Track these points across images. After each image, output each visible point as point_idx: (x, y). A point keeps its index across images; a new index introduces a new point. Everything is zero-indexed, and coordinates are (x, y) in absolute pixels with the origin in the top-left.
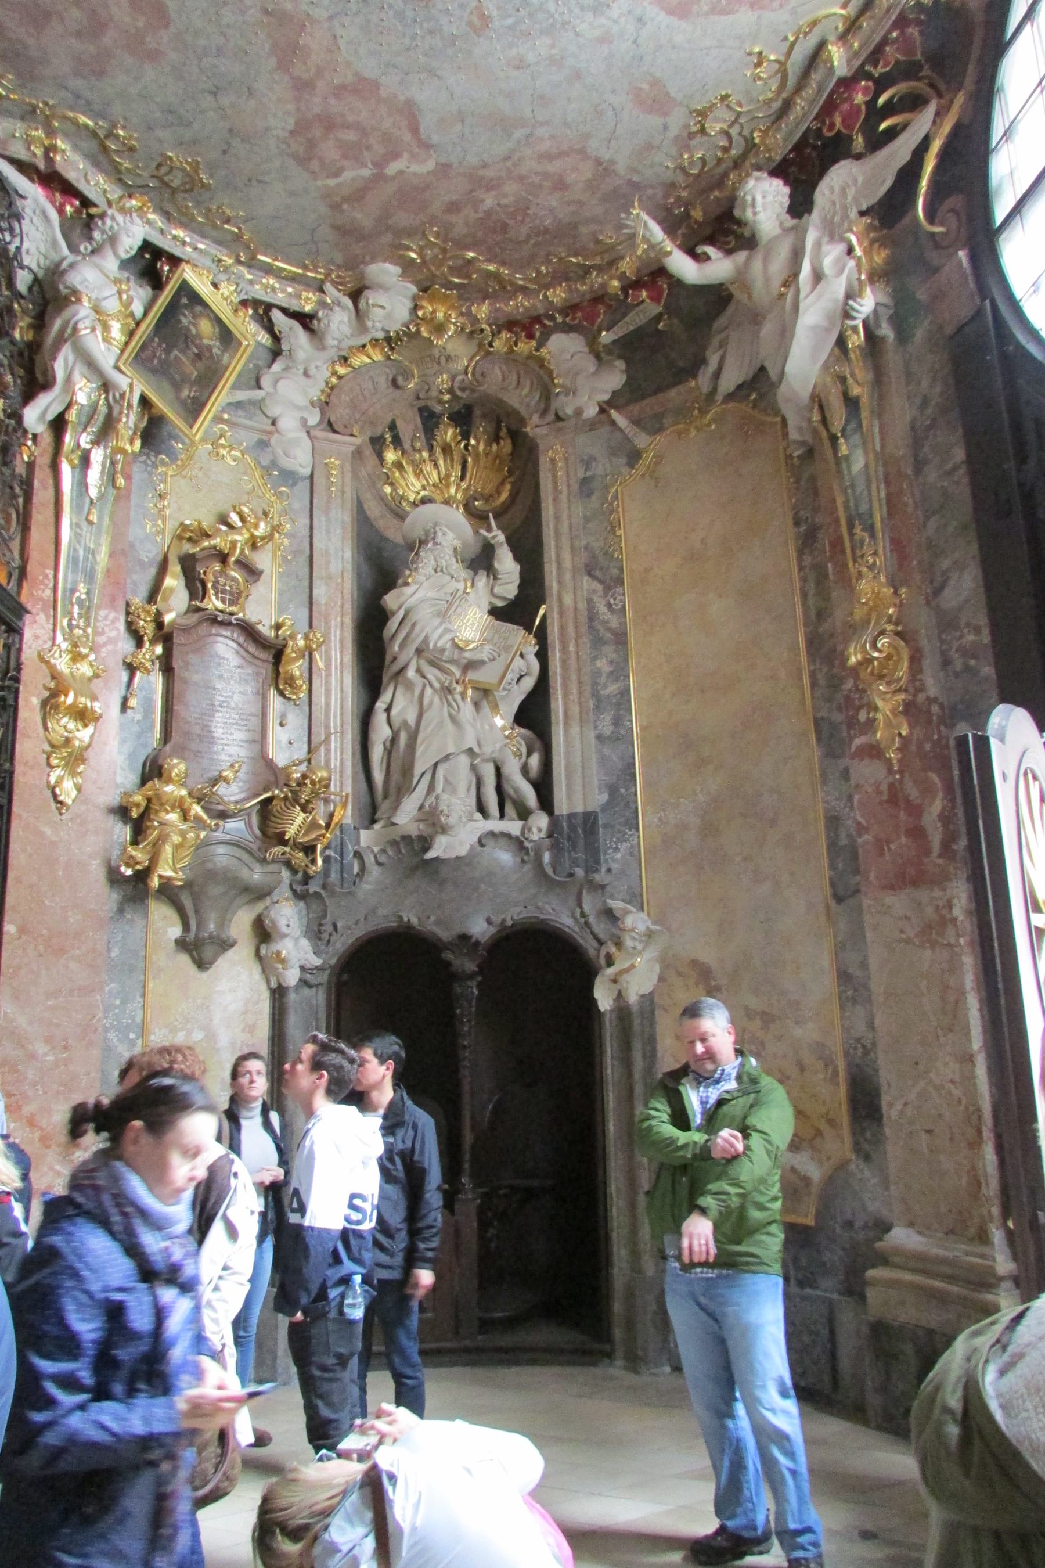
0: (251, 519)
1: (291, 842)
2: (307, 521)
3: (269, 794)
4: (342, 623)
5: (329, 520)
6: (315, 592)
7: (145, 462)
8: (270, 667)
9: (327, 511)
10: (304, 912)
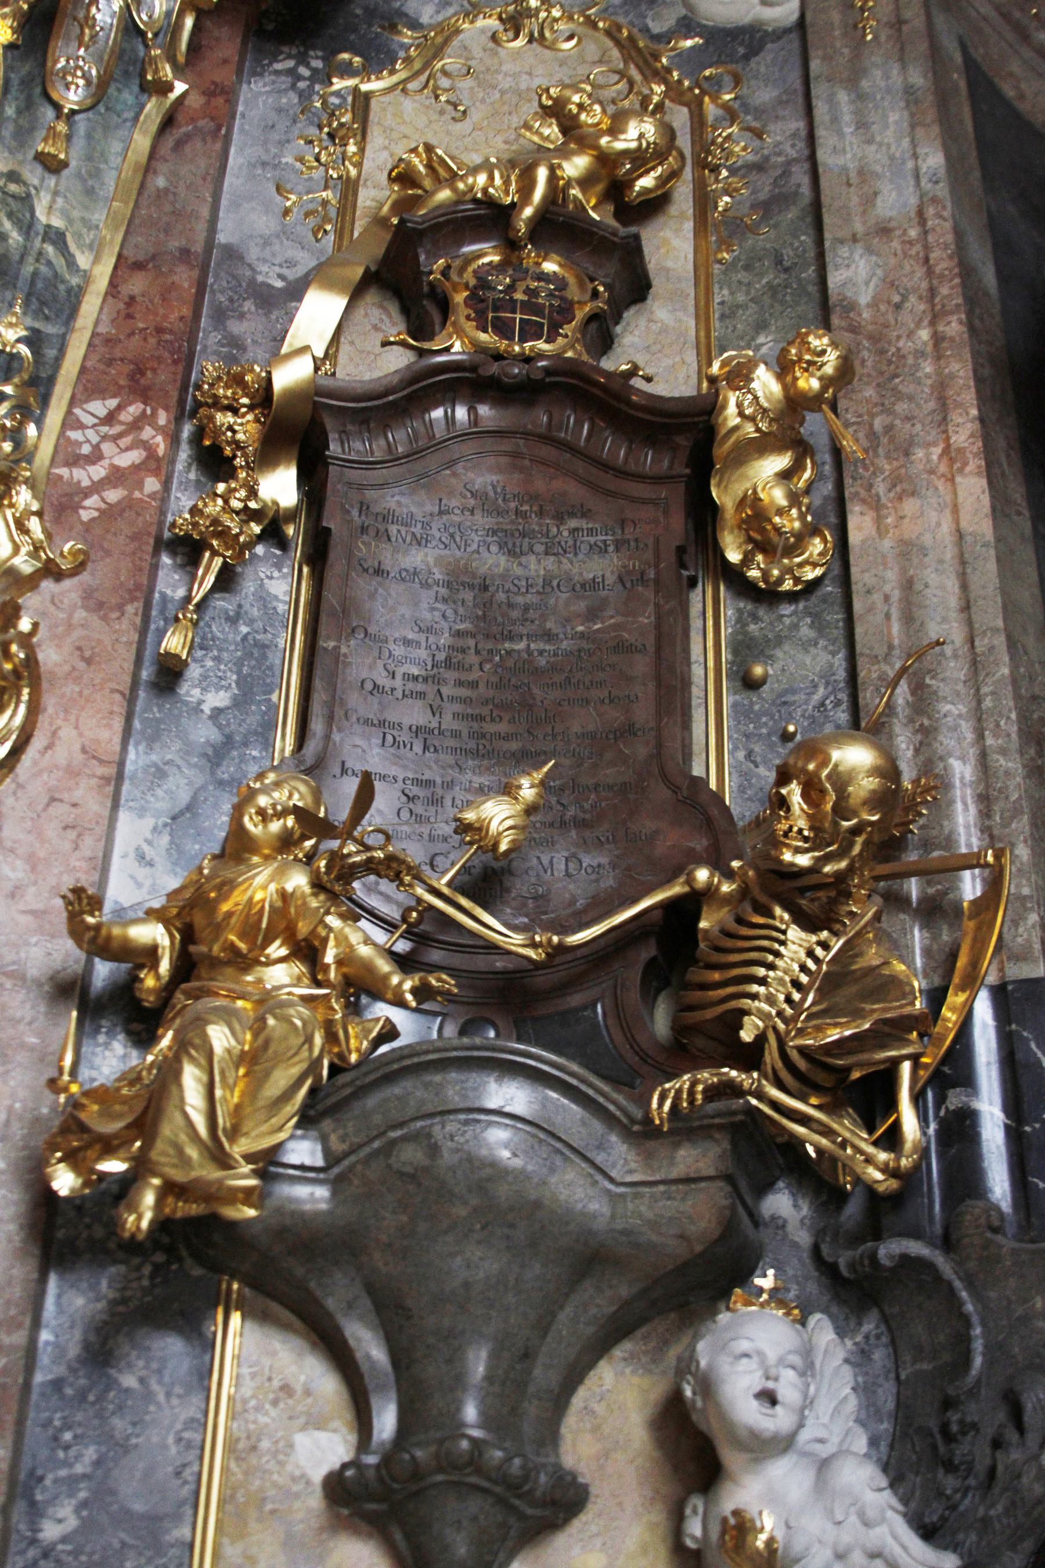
0: (593, 117)
1: (771, 1055)
2: (799, 125)
3: (677, 889)
4: (938, 339)
5: (861, 97)
6: (835, 279)
7: (291, 72)
8: (675, 496)
9: (853, 80)
10: (879, 1355)
